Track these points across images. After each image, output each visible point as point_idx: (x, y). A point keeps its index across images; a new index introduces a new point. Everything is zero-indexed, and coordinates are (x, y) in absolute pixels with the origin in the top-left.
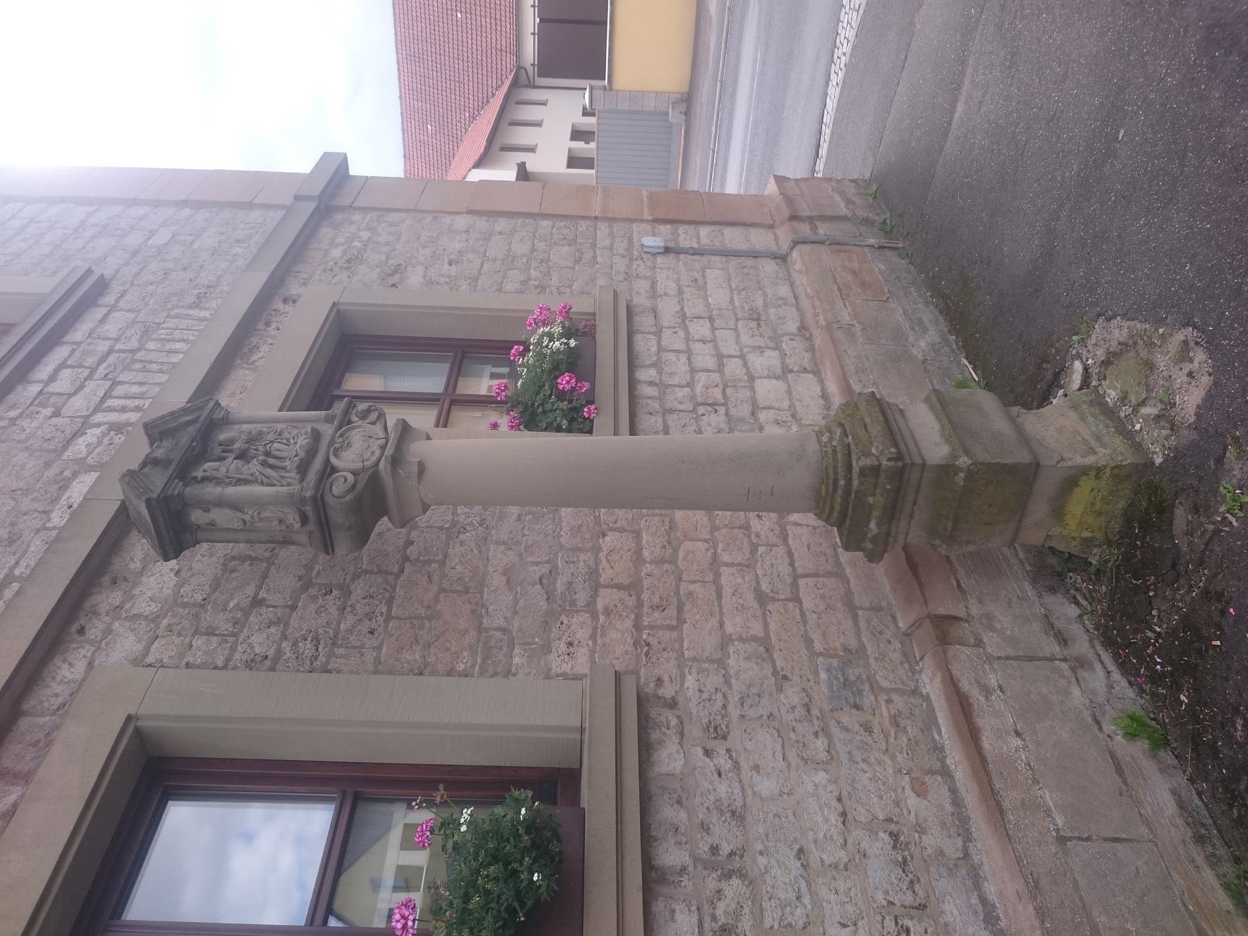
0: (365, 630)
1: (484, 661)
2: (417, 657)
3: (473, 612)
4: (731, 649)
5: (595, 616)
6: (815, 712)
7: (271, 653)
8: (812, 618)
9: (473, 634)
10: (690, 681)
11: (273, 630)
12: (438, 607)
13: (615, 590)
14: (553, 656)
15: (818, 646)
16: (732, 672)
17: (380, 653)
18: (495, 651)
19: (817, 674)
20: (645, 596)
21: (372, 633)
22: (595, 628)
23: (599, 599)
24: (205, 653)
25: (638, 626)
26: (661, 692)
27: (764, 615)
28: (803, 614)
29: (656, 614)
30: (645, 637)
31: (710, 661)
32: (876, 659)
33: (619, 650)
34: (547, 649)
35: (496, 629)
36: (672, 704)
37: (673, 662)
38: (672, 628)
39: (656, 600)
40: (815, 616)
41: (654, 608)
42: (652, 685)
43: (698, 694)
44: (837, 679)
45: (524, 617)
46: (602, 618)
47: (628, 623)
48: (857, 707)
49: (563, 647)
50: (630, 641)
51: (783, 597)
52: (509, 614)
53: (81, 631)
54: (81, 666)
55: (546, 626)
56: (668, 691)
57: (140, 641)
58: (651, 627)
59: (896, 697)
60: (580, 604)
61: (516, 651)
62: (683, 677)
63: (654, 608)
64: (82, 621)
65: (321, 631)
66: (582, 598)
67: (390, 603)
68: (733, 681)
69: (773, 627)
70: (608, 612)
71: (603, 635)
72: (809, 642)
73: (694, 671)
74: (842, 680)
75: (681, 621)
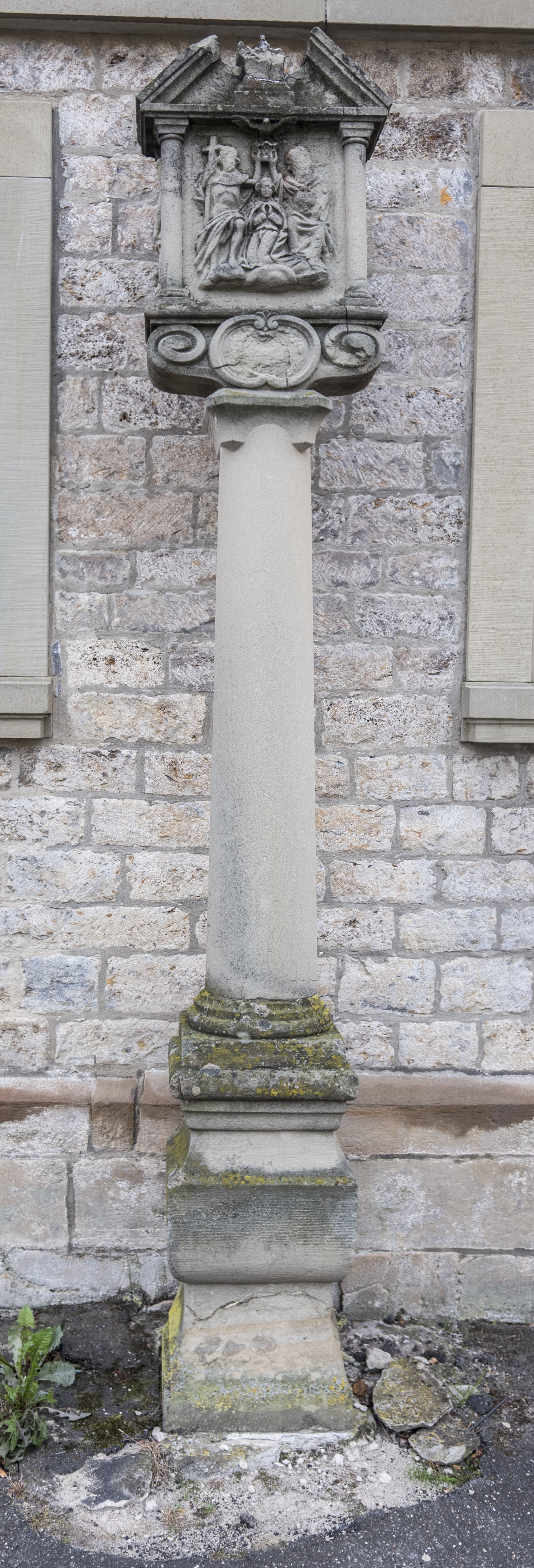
0: (126, 409)
1: (83, 558)
2: (86, 479)
3: (162, 538)
4: (108, 856)
5: (156, 691)
6: (19, 940)
7: (87, 303)
8: (165, 962)
9: (124, 542)
10: (58, 802)
11: (123, 295)
12: (169, 493)
13: (202, 717)
14: (92, 641)
15: (115, 962)
16: (73, 853)
17: (92, 432)
18: (97, 570)
19: (74, 953)
20: (193, 755)
21: (124, 416)
22: (138, 691)
23: (187, 696)
24: (85, 224)
25: (142, 743)
26: (40, 767)
27: (166, 904)
28: (168, 952)
29: (161, 768)
30: (125, 752)
31: (89, 828)
32: (98, 1028)
33: (105, 721)
34: (104, 632)
35: (133, 569)
36: (24, 780)
37: (84, 785)
38: (140, 786)
39: (186, 769)
40: (167, 967)
41: (174, 766)
42: (51, 757)
43: (39, 810)
44: (67, 975)
45: (154, 601)
46: (155, 700)
47: (146, 733)
48: (29, 990)
49: (107, 652)
50: (118, 734)
51: (198, 932)
52: (158, 582)
53: (118, 59)
54: (60, 82)
55: (139, 630)
56: (40, 774)
57: (101, 138)
58: (141, 762)
59: (40, 1039)
60: (177, 672)
61: (99, 596)
62: (66, 794)
63: (174, 766)
64: (132, 54)
65: (124, 354)
66: (190, 674)
67: (174, 430)
68: (60, 853)
69: (147, 912)
70: (163, 707)
71: (128, 702)
72: (126, 951)
73: (71, 808)
74: (66, 980)
75: (152, 799)
